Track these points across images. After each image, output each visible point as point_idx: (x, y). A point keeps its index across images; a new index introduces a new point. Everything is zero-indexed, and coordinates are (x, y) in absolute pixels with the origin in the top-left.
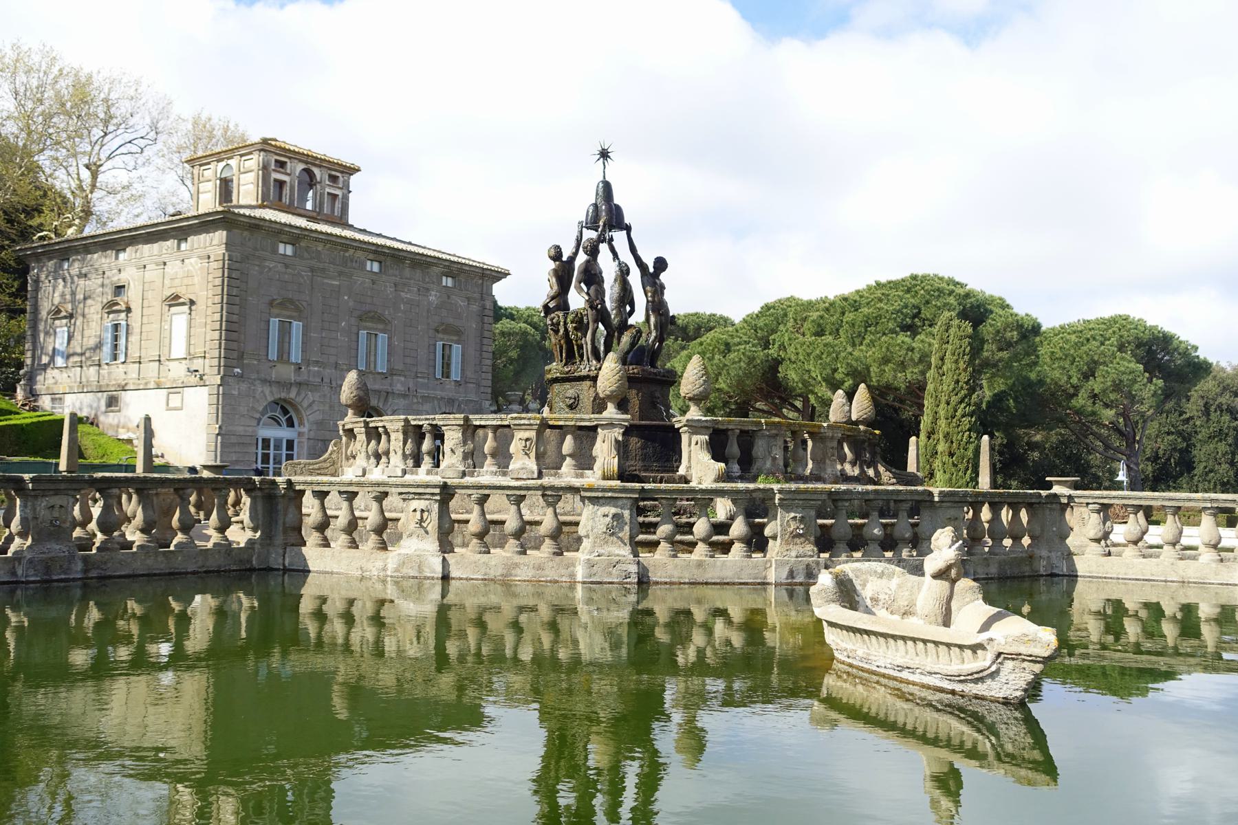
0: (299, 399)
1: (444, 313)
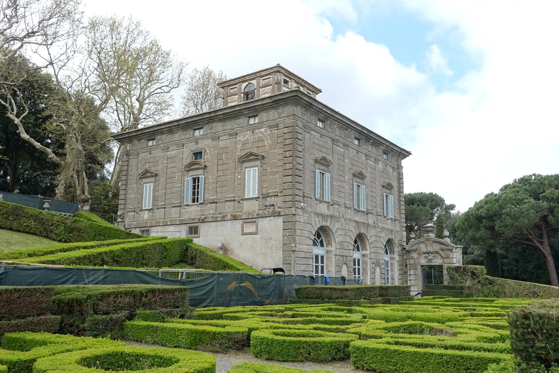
0: (331, 227)
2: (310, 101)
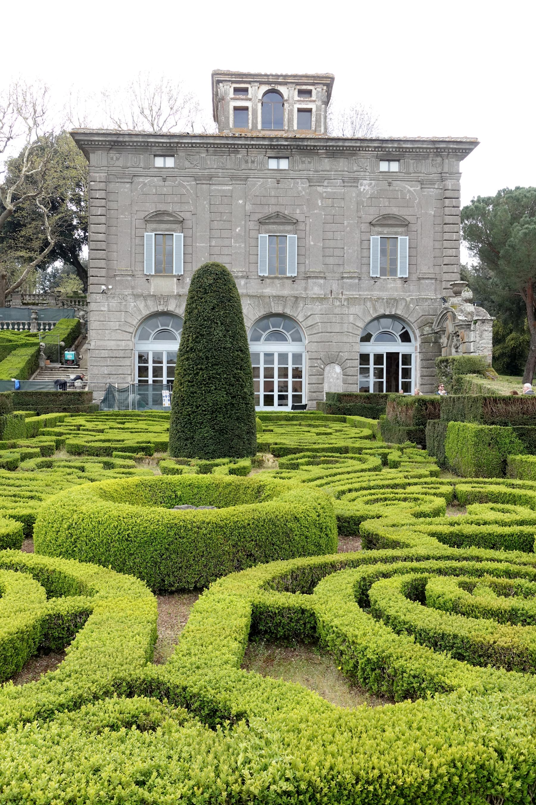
1: (384, 202)
2: (109, 139)
